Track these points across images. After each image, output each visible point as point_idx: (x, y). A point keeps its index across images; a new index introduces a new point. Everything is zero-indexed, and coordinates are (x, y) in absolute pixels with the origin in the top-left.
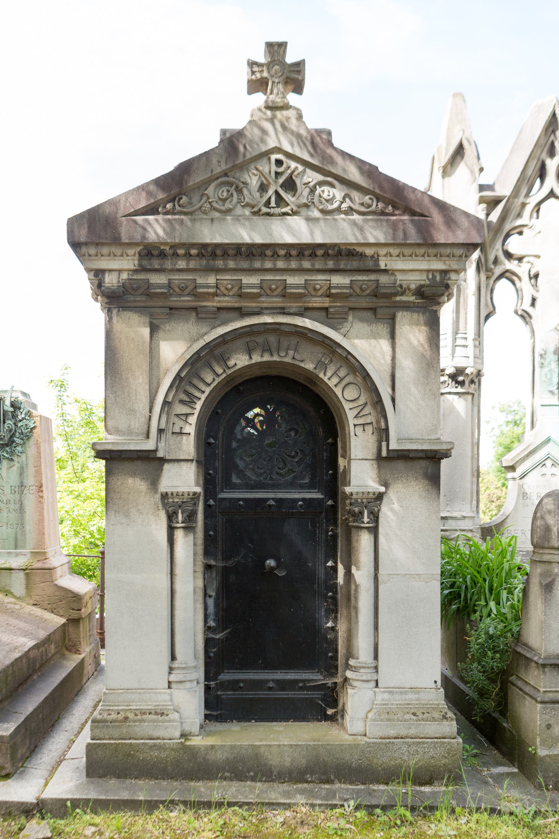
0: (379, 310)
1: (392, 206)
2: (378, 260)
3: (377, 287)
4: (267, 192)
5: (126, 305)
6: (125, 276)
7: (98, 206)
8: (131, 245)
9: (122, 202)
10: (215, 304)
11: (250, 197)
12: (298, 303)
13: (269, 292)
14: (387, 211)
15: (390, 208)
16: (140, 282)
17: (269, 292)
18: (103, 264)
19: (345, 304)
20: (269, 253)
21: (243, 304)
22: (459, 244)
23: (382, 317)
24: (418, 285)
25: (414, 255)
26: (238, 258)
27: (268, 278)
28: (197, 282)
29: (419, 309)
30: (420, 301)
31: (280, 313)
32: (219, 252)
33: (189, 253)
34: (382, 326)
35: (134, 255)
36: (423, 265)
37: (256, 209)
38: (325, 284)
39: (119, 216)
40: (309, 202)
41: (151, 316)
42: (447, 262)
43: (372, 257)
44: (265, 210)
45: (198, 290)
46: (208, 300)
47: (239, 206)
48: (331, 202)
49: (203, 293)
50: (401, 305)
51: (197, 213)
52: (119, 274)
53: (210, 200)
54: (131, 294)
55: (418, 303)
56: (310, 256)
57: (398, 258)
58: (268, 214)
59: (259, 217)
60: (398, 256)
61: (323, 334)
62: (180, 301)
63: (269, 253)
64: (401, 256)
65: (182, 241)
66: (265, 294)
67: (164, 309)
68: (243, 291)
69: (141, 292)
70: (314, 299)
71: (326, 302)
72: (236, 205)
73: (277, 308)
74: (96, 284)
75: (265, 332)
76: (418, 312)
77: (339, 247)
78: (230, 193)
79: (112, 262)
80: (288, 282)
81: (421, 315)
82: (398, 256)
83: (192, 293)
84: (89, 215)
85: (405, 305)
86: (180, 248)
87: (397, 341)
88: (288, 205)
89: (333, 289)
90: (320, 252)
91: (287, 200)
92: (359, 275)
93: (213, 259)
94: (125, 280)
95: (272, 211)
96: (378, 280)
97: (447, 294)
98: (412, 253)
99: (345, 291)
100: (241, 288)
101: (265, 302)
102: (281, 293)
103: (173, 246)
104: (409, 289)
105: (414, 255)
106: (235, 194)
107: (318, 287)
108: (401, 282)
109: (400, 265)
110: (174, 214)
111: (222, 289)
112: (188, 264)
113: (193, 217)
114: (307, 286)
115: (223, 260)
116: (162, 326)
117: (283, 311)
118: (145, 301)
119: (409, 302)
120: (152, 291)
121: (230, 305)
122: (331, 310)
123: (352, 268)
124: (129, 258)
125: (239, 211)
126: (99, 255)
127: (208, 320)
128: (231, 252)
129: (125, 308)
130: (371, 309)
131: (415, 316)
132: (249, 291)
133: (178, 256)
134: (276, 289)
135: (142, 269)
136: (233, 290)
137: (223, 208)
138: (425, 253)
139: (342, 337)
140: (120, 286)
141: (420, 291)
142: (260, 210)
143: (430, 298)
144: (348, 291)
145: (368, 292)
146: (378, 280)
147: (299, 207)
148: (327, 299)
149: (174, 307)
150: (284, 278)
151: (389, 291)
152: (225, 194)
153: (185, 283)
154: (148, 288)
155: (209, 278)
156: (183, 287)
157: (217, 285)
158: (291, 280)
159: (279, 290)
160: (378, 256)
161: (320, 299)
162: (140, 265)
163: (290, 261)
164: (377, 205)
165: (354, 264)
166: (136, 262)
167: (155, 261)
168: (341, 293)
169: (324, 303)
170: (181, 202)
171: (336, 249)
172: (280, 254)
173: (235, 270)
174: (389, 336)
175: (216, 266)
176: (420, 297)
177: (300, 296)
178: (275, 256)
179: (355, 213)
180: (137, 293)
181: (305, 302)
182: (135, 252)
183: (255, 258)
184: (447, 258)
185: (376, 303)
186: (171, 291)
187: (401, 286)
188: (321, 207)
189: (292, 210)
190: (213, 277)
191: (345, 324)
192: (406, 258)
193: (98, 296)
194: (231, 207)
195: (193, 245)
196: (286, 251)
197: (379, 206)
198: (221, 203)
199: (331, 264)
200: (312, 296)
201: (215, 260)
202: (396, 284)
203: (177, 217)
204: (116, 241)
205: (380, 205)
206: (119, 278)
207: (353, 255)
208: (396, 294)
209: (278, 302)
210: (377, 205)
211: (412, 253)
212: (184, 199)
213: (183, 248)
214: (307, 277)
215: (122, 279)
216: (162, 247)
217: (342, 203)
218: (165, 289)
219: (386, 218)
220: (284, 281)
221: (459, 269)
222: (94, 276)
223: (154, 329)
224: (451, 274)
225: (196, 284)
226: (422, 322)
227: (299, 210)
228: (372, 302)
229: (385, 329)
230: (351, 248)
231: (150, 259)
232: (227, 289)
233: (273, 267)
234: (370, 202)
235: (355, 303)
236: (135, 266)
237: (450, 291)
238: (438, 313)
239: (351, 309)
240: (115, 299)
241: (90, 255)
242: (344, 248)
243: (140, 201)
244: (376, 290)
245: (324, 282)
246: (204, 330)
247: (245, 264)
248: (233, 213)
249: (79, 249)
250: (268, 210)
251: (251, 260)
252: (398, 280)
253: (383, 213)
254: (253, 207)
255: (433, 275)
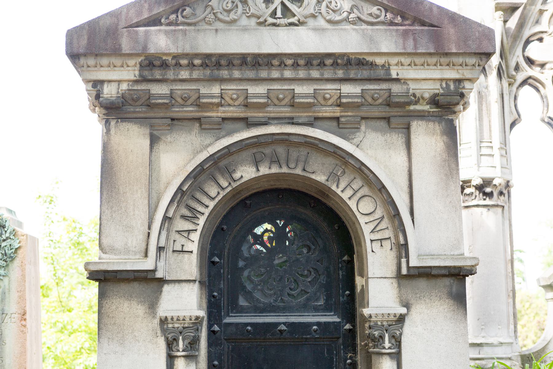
0: (392, 120)
1: (401, 17)
2: (389, 69)
3: (390, 96)
4: (273, 3)
5: (126, 116)
6: (124, 86)
7: (99, 18)
8: (130, 55)
9: (123, 13)
10: (219, 114)
11: (256, 8)
12: (308, 112)
13: (276, 102)
14: (396, 22)
15: (399, 18)
16: (141, 92)
17: (276, 102)
18: (102, 75)
19: (357, 114)
20: (276, 62)
21: (249, 114)
22: (471, 53)
23: (397, 127)
24: (432, 94)
25: (426, 64)
26: (244, 67)
27: (275, 88)
28: (201, 92)
29: (434, 118)
30: (435, 110)
31: (289, 123)
32: (223, 62)
33: (192, 63)
34: (397, 135)
35: (135, 65)
36: (436, 74)
37: (261, 20)
38: (335, 93)
39: (120, 27)
40: (316, 13)
41: (152, 126)
42: (460, 71)
43: (383, 66)
44: (271, 20)
45: (201, 100)
46: (213, 111)
47: (244, 16)
48: (339, 12)
49: (207, 103)
50: (416, 114)
51: (200, 24)
52: (119, 85)
53: (215, 11)
54: (130, 105)
55: (433, 111)
56: (319, 65)
57: (410, 67)
58: (274, 25)
59: (264, 28)
60: (409, 65)
61: (335, 145)
62: (182, 111)
63: (276, 62)
64: (413, 65)
65: (185, 51)
66: (272, 104)
67: (166, 119)
68: (249, 101)
69: (141, 103)
70: (324, 109)
71: (337, 112)
72: (241, 16)
73: (285, 118)
74: (94, 95)
75: (272, 143)
76: (434, 121)
77: (348, 56)
78: (235, 4)
79: (111, 73)
80: (296, 92)
81: (437, 124)
82: (409, 65)
83: (195, 104)
84: (89, 27)
85: (419, 114)
86: (183, 58)
87: (413, 151)
88: (294, 15)
89: (343, 98)
90: (329, 62)
91: (293, 10)
92: (371, 84)
93: (217, 69)
94: (125, 90)
95: (278, 21)
96: (390, 90)
97: (462, 103)
98: (424, 62)
99: (356, 100)
100: (247, 98)
101: (272, 112)
102: (289, 103)
103: (176, 57)
104: (423, 98)
105: (426, 64)
106: (240, 5)
107: (328, 96)
108: (414, 91)
109: (411, 74)
110: (177, 25)
111: (227, 99)
112: (191, 74)
113: (197, 28)
114: (316, 96)
115: (228, 70)
116: (163, 138)
117: (291, 121)
118: (145, 112)
119: (423, 111)
120: (153, 101)
121: (235, 115)
122: (342, 119)
123: (362, 77)
124: (129, 68)
125: (244, 21)
126: (98, 66)
127: (212, 131)
128: (236, 62)
129: (124, 119)
130: (385, 118)
131: (431, 125)
132: (255, 100)
133: (181, 66)
134: (283, 99)
135: (143, 80)
136: (239, 99)
137: (227, 19)
138: (437, 62)
139: (355, 147)
140: (119, 97)
141: (434, 100)
142: (266, 21)
143: (445, 107)
144: (359, 100)
145: (380, 101)
146: (390, 90)
147: (306, 17)
148: (338, 108)
149: (176, 117)
150: (292, 87)
151: (402, 100)
152: (230, 5)
153: (188, 93)
154: (149, 98)
155: (214, 88)
156: (185, 97)
157: (221, 95)
158: (299, 89)
159: (287, 100)
160: (389, 65)
161: (331, 109)
162: (140, 75)
163: (298, 70)
164: (386, 16)
165: (365, 73)
166: (137, 73)
167: (157, 72)
168: (352, 102)
169: (334, 112)
170: (185, 13)
171: (345, 58)
172: (287, 64)
173: (240, 80)
174: (404, 146)
175: (221, 75)
176: (434, 106)
177: (309, 106)
178: (282, 65)
179: (363, 24)
180: (137, 104)
181: (314, 112)
182: (136, 63)
183: (261, 68)
184: (460, 67)
185: (389, 112)
186: (173, 102)
187: (414, 95)
188: (328, 18)
189: (299, 21)
190: (218, 87)
191: (358, 134)
192: (418, 67)
193: (96, 107)
194: (236, 17)
195: (197, 55)
196: (293, 61)
197: (388, 16)
198: (225, 14)
199: (340, 74)
200: (322, 105)
201: (220, 70)
202: (408, 93)
203: (181, 27)
204: (117, 52)
205: (389, 16)
206: (118, 89)
207: (363, 65)
208: (409, 104)
209: (286, 111)
210: (386, 16)
211: (424, 62)
212: (188, 10)
213: (186, 58)
214: (316, 87)
215: (121, 90)
216: (164, 58)
217: (350, 13)
218: (167, 99)
219: (395, 28)
220: (292, 91)
221: (474, 78)
222: (93, 87)
223: (154, 140)
224: (465, 83)
225: (200, 94)
226: (439, 131)
227: (305, 20)
228: (385, 112)
229: (400, 138)
230: (361, 57)
231: (151, 70)
232: (232, 99)
233: (280, 76)
234: (378, 12)
235: (367, 112)
236: (135, 76)
237: (465, 100)
238: (454, 123)
239: (363, 118)
240: (114, 111)
241: (88, 66)
242: (353, 57)
243: (142, 12)
244: (388, 99)
245: (334, 91)
246: (208, 141)
247: (251, 74)
248: (238, 23)
249: (77, 60)
250: (274, 21)
251: (257, 70)
252: (411, 89)
253: (392, 23)
254: (259, 18)
255: (446, 84)
